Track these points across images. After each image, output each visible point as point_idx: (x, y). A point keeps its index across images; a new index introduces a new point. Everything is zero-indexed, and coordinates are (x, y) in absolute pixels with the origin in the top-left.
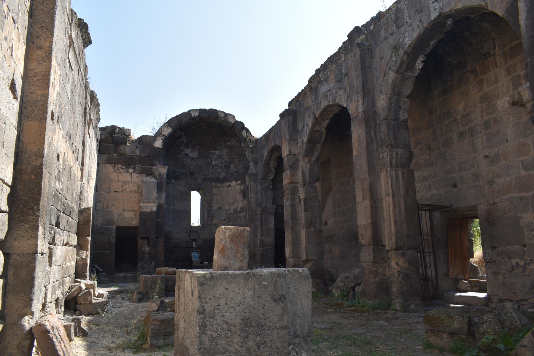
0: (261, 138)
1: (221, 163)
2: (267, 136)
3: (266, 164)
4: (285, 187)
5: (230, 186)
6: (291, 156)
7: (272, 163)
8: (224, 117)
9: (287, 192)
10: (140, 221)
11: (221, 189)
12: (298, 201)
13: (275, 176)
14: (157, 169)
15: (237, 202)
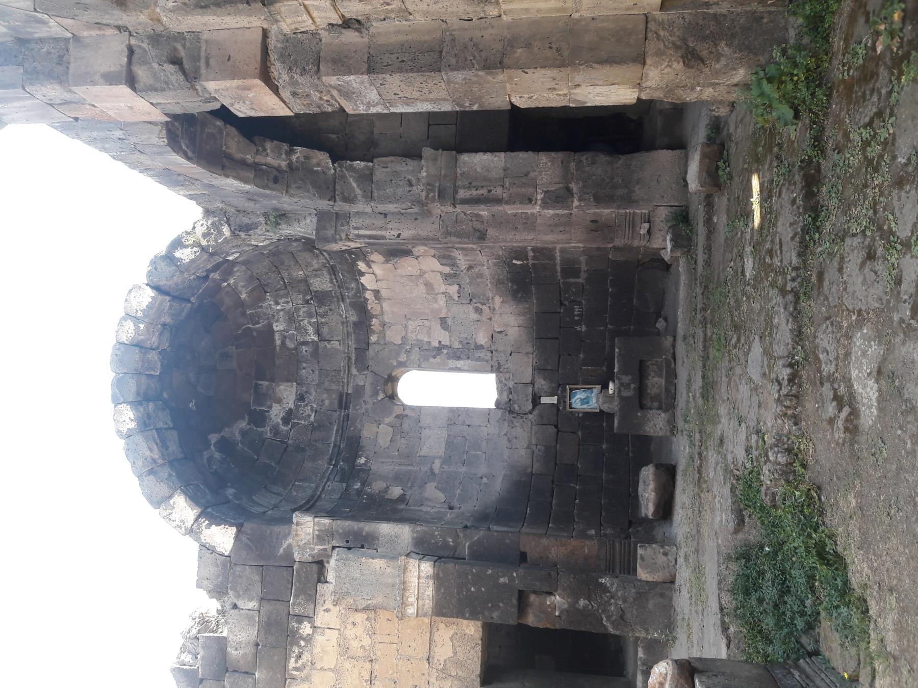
0: (191, 197)
1: (310, 316)
2: (170, 178)
3: (276, 180)
4: (299, 107)
5: (376, 293)
6: (141, 73)
7: (269, 159)
8: (136, 320)
9: (315, 95)
10: (464, 617)
11: (387, 319)
12: (350, 36)
13: (321, 148)
14: (302, 548)
15: (422, 274)
